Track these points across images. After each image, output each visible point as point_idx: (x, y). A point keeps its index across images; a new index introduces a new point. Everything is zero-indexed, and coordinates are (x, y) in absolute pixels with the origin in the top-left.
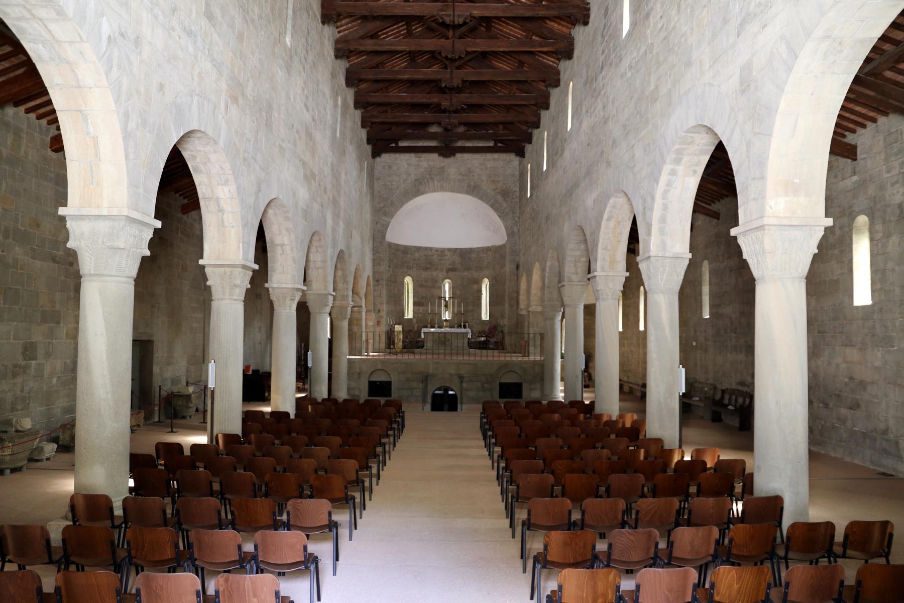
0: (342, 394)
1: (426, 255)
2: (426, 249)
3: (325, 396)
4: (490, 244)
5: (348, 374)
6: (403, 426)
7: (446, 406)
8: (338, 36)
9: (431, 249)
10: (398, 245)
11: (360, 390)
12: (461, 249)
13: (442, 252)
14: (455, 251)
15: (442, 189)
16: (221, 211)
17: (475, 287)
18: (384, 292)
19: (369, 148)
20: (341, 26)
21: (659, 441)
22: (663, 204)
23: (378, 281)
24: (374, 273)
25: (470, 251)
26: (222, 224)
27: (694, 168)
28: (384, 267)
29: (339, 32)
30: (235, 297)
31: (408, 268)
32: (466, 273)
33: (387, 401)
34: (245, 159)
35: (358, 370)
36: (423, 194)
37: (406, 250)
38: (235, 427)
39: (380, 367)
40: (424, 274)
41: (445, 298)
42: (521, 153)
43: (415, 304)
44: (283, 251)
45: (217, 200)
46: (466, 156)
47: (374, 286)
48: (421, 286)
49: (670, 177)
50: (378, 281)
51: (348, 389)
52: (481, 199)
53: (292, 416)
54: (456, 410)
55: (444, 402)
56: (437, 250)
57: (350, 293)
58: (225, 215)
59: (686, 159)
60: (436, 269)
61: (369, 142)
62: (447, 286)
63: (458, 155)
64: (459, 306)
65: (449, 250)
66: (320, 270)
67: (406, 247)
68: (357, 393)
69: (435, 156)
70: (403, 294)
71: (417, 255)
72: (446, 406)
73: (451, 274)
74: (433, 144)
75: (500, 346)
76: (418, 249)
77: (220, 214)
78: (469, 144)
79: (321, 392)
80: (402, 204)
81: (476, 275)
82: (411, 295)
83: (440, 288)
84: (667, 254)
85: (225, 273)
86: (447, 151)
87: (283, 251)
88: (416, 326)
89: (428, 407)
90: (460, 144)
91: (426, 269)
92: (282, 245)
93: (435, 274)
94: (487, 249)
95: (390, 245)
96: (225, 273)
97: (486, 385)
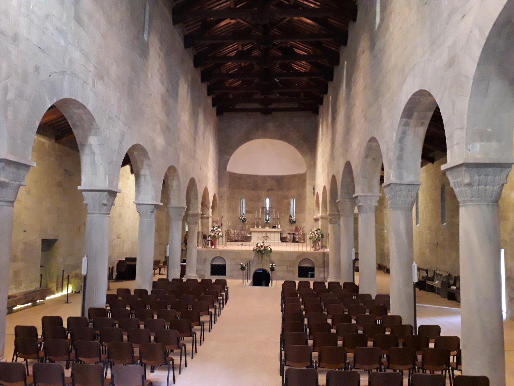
0: (191, 274)
2: (254, 176)
3: (178, 276)
4: (296, 173)
5: (197, 260)
6: (227, 298)
7: (264, 282)
8: (187, 33)
9: (257, 176)
10: (235, 174)
11: (205, 271)
12: (277, 176)
15: (264, 137)
16: (93, 153)
18: (226, 205)
19: (214, 110)
20: (189, 26)
21: (398, 318)
22: (400, 147)
23: (221, 197)
24: (219, 193)
26: (93, 163)
27: (422, 121)
28: (225, 189)
29: (187, 30)
30: (103, 212)
32: (280, 192)
33: (216, 280)
34: (110, 118)
35: (204, 257)
36: (251, 140)
38: (100, 301)
39: (219, 256)
41: (266, 208)
42: (316, 112)
44: (145, 180)
45: (90, 145)
46: (280, 114)
47: (219, 200)
48: (251, 200)
49: (404, 127)
50: (221, 197)
51: (197, 271)
52: (289, 143)
53: (149, 293)
54: (268, 286)
55: (261, 279)
57: (200, 206)
58: (96, 156)
59: (415, 114)
61: (214, 105)
63: (274, 113)
64: (276, 213)
65: (270, 177)
66: (176, 192)
67: (241, 175)
68: (203, 273)
69: (259, 114)
70: (239, 205)
72: (264, 282)
73: (270, 192)
74: (257, 106)
75: (302, 240)
76: (249, 176)
77: (93, 155)
78: (282, 106)
79: (175, 274)
80: (238, 147)
82: (244, 206)
83: (264, 202)
84: (403, 183)
85: (96, 195)
86: (266, 112)
87: (145, 180)
88: (247, 227)
89: (250, 281)
90: (274, 106)
91: (254, 189)
92: (144, 176)
93: (260, 192)
94: (294, 176)
95: (230, 174)
96: (96, 195)
97: (289, 268)
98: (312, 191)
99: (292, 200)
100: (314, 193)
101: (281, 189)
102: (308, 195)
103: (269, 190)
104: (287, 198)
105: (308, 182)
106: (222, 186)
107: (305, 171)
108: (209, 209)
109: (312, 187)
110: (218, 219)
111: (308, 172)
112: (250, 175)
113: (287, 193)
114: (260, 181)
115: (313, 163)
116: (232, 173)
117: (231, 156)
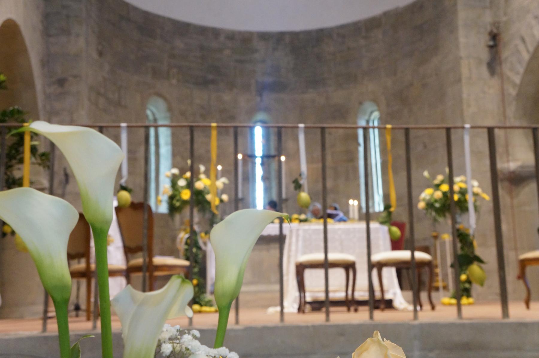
1: (202, 48)
2: (203, 30)
9: (216, 32)
12: (294, 35)
13: (244, 41)
14: (277, 39)
23: (61, 82)
25: (319, 36)
31: (156, 73)
32: (310, 95)
40: (200, 97)
47: (48, 97)
56: (232, 36)
60: (231, 86)
65: (264, 36)
67: (147, 16)
71: (179, 44)
73: (268, 98)
76: (183, 29)
81: (338, 96)
91: (204, 83)
93: (227, 97)
94: (372, 24)
98: (485, 55)
100: (494, 64)
101: (315, 82)
102: (465, 72)
103: (262, 89)
104: (343, 113)
105: (463, 15)
106: (66, 32)
109: (485, 40)
113: (338, 96)
114: (227, 52)
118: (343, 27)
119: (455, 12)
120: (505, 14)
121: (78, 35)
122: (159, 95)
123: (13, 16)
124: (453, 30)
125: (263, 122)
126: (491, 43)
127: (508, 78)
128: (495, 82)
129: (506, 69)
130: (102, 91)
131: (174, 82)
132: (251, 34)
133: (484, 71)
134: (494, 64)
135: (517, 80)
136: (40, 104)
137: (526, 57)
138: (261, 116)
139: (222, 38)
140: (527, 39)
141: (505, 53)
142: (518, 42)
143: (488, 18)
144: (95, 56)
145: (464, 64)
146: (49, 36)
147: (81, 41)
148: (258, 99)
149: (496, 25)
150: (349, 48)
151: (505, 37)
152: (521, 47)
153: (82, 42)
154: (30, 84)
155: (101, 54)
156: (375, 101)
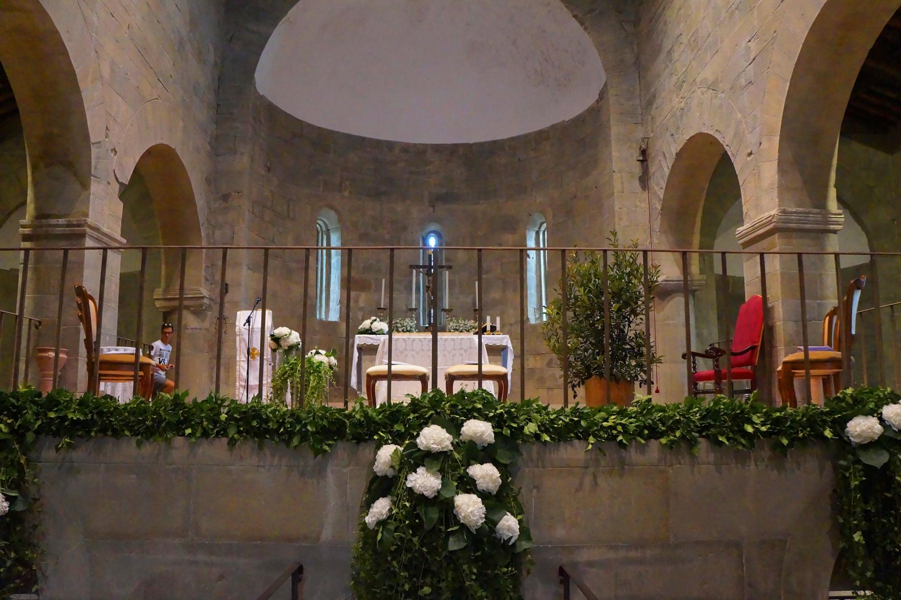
2: (378, 144)
4: (545, 124)
9: (390, 145)
13: (418, 154)
17: (509, 239)
23: (225, 198)
25: (492, 148)
37: (323, 141)
43: (347, 284)
48: (364, 237)
56: (406, 148)
62: (432, 242)
65: (438, 149)
91: (377, 195)
93: (400, 207)
94: (541, 137)
98: (637, 169)
99: (533, 234)
100: (644, 180)
102: (617, 186)
105: (615, 130)
107: (590, 100)
108: (85, 186)
109: (637, 155)
110: (205, 292)
111: (611, 92)
112: (364, 139)
115: (629, 57)
116: (288, 116)
117: (274, 25)
118: (512, 139)
119: (610, 129)
120: (652, 131)
121: (242, 154)
122: (332, 208)
123: (175, 142)
124: (608, 144)
125: (434, 232)
126: (641, 158)
127: (655, 192)
128: (645, 195)
129: (652, 183)
130: (269, 204)
131: (346, 194)
132: (426, 145)
133: (637, 182)
134: (644, 180)
135: (661, 194)
136: (202, 219)
137: (667, 172)
138: (434, 227)
139: (397, 151)
140: (667, 155)
141: (652, 169)
142: (661, 158)
143: (640, 134)
144: (263, 172)
145: (616, 176)
146: (218, 156)
147: (244, 160)
148: (431, 209)
149: (646, 140)
150: (519, 160)
151: (652, 152)
152: (663, 164)
153: (246, 159)
154: (190, 200)
155: (269, 169)
156: (543, 212)
